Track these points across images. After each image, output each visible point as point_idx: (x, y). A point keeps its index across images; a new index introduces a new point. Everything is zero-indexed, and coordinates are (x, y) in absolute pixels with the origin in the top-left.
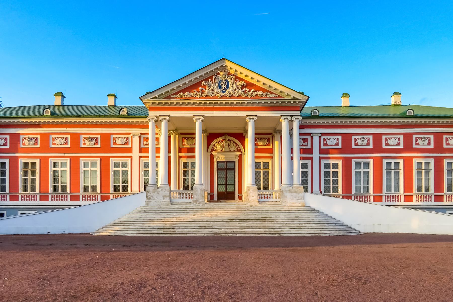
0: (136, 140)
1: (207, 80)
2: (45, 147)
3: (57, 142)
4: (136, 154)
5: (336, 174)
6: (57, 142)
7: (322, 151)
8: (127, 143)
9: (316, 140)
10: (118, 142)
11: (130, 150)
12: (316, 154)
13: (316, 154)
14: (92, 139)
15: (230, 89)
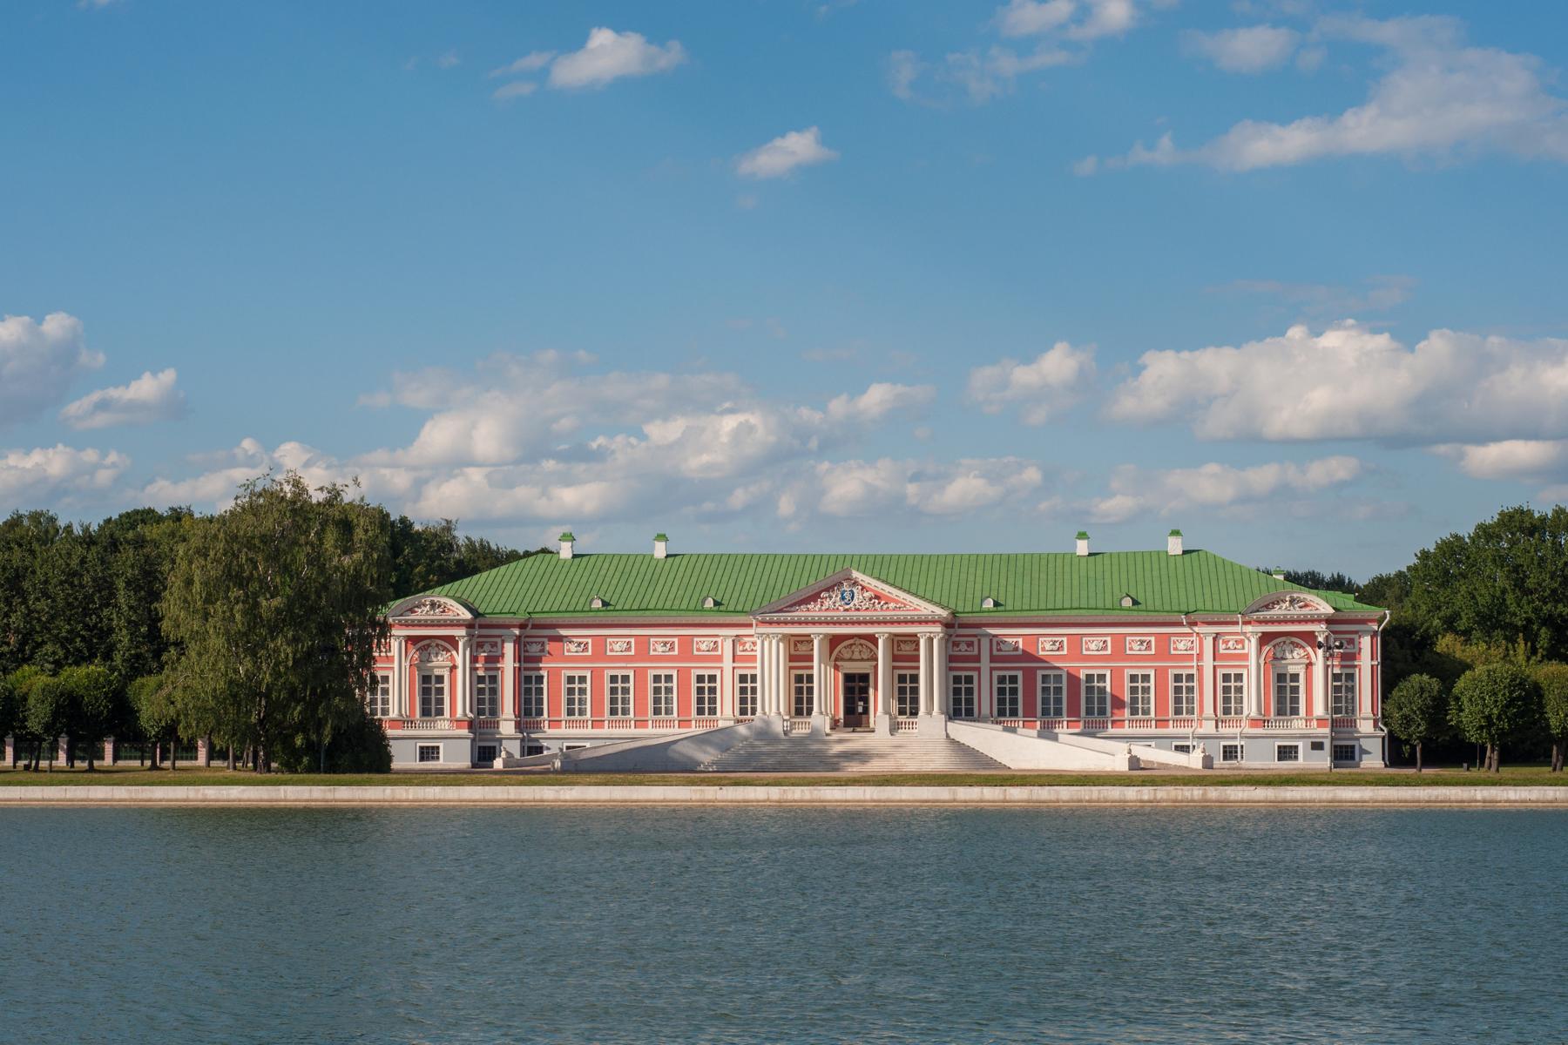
0: (728, 644)
1: (827, 590)
2: (600, 654)
3: (617, 647)
4: (728, 663)
5: (1014, 691)
6: (617, 647)
7: (993, 659)
8: (715, 649)
9: (985, 643)
10: (703, 647)
11: (719, 659)
12: (985, 664)
13: (985, 664)
14: (665, 644)
15: (856, 601)
